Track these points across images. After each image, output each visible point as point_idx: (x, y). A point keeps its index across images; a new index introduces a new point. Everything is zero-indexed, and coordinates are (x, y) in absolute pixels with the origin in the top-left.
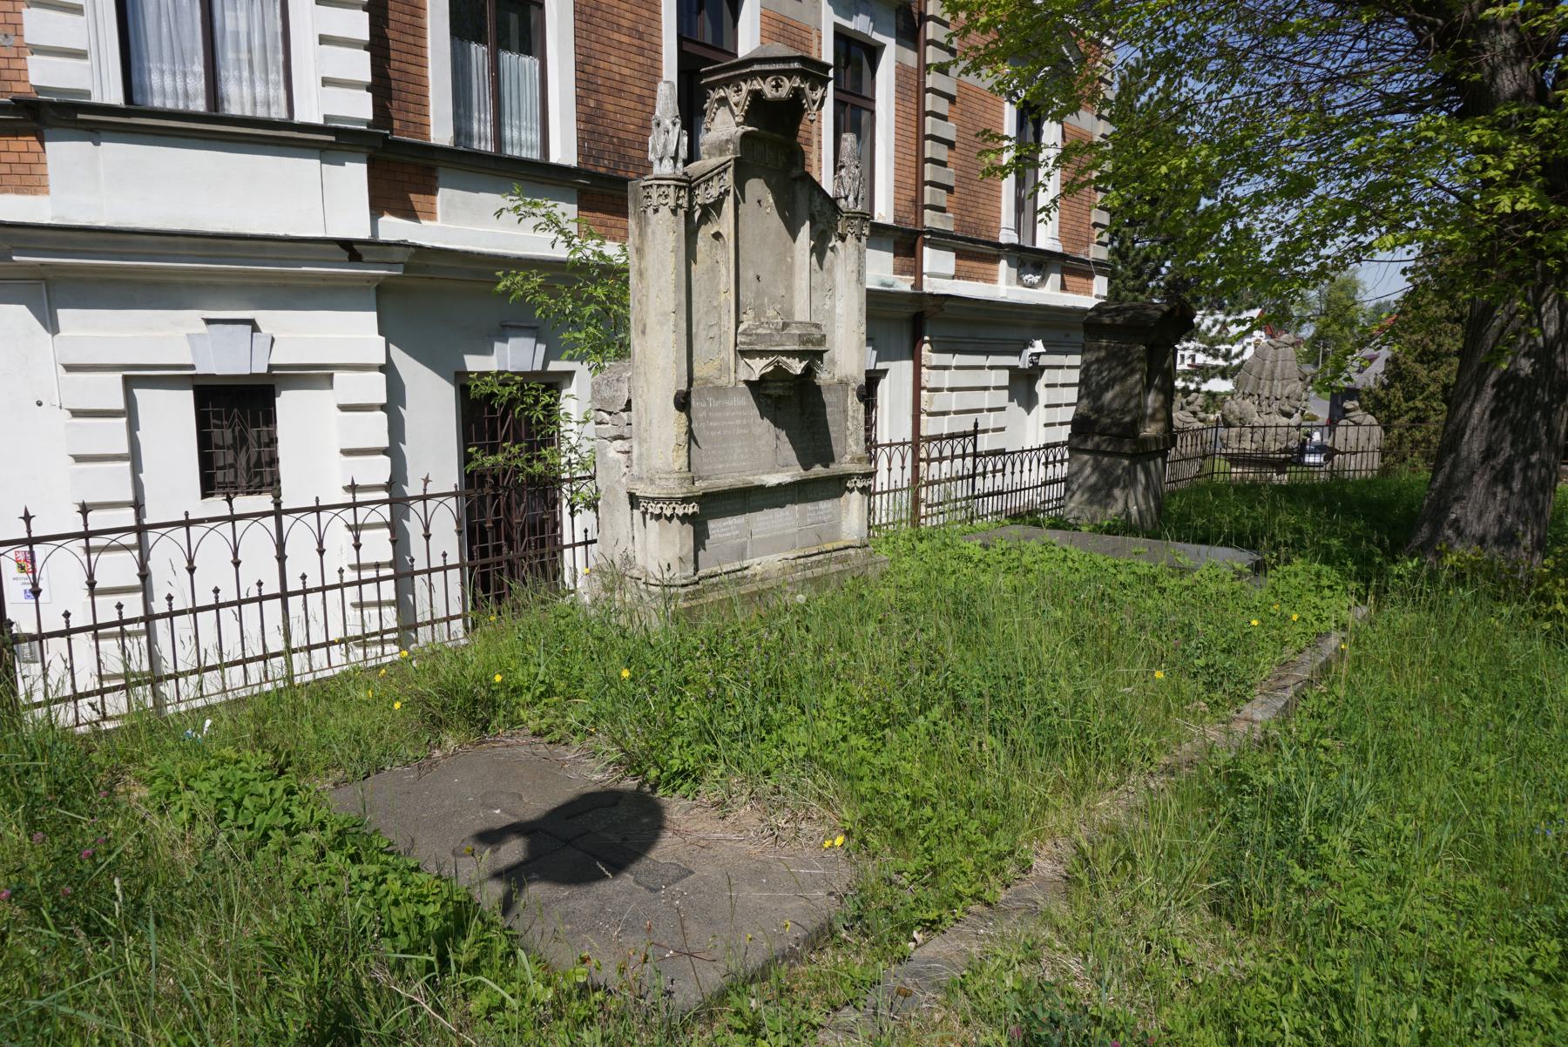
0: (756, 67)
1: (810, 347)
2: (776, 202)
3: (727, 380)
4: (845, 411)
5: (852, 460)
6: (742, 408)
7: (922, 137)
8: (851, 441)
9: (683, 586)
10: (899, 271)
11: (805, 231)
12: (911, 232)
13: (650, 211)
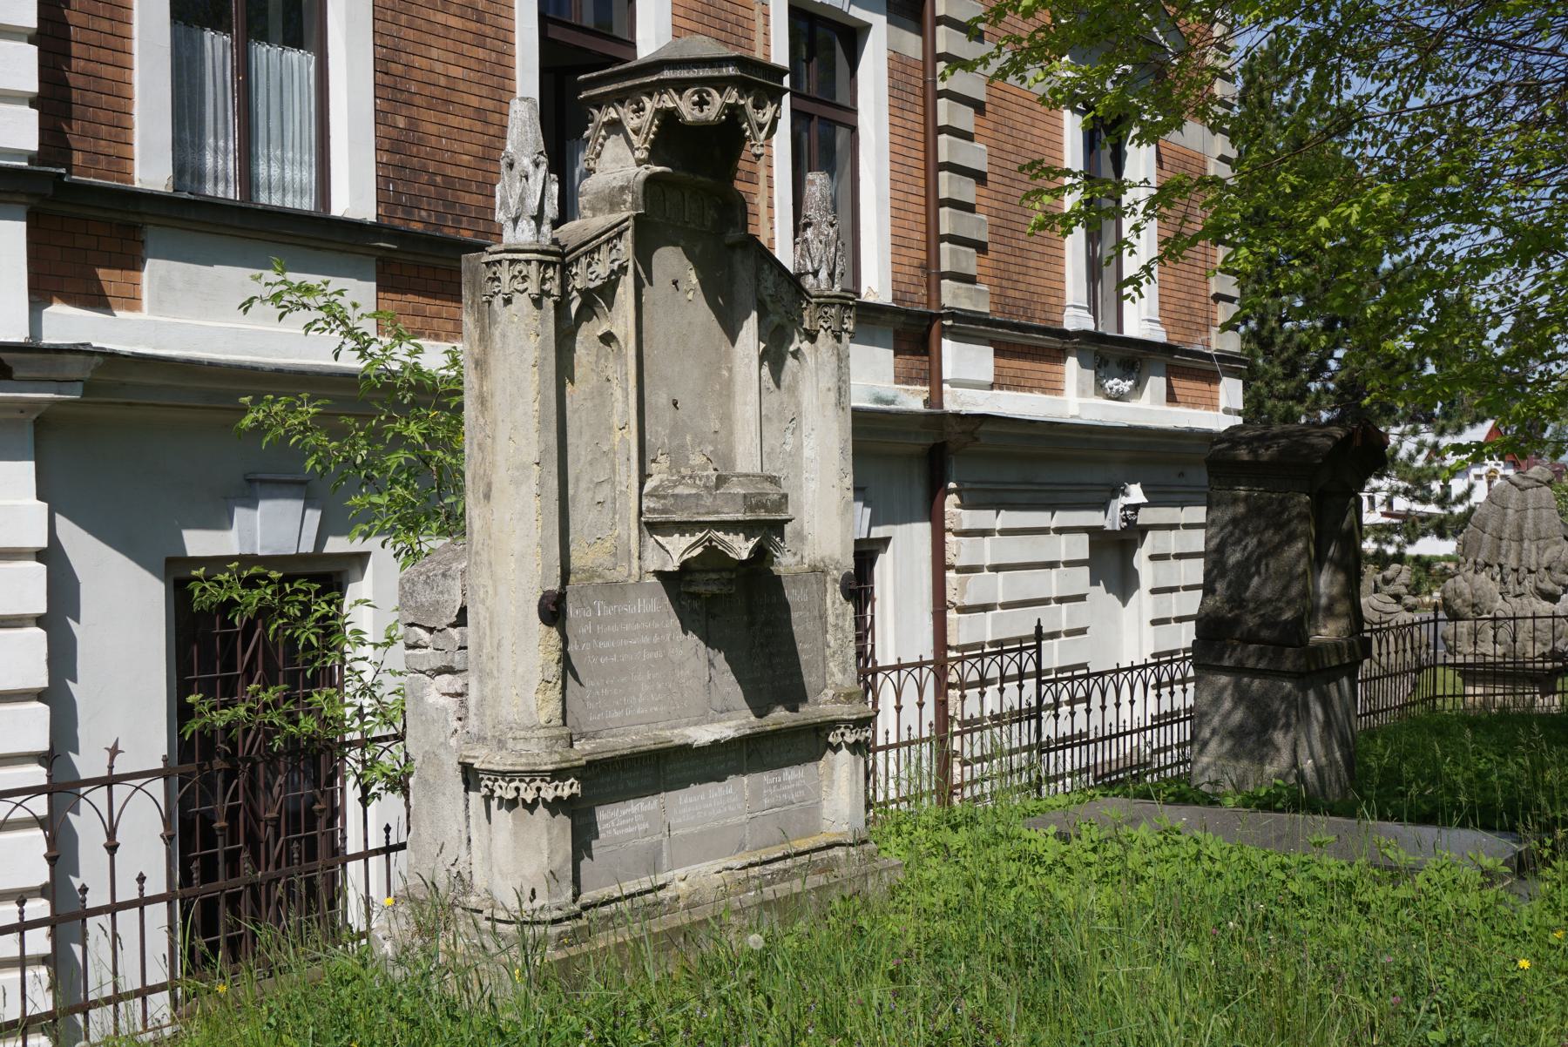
0: (667, 74)
2: (701, 282)
3: (627, 571)
4: (822, 617)
5: (836, 698)
6: (651, 617)
7: (933, 167)
8: (833, 666)
9: (555, 922)
10: (903, 378)
11: (750, 328)
12: (921, 315)
13: (498, 302)
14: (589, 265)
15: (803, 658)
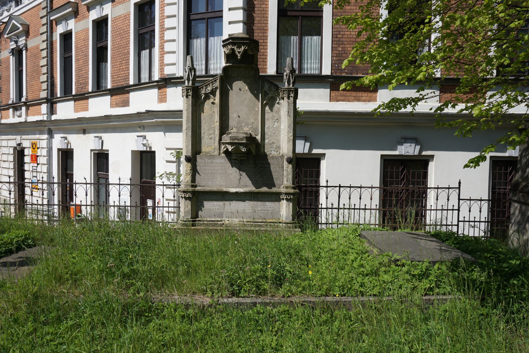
1: (236, 141)
6: (222, 163)
8: (285, 180)
14: (206, 88)
15: (274, 177)
